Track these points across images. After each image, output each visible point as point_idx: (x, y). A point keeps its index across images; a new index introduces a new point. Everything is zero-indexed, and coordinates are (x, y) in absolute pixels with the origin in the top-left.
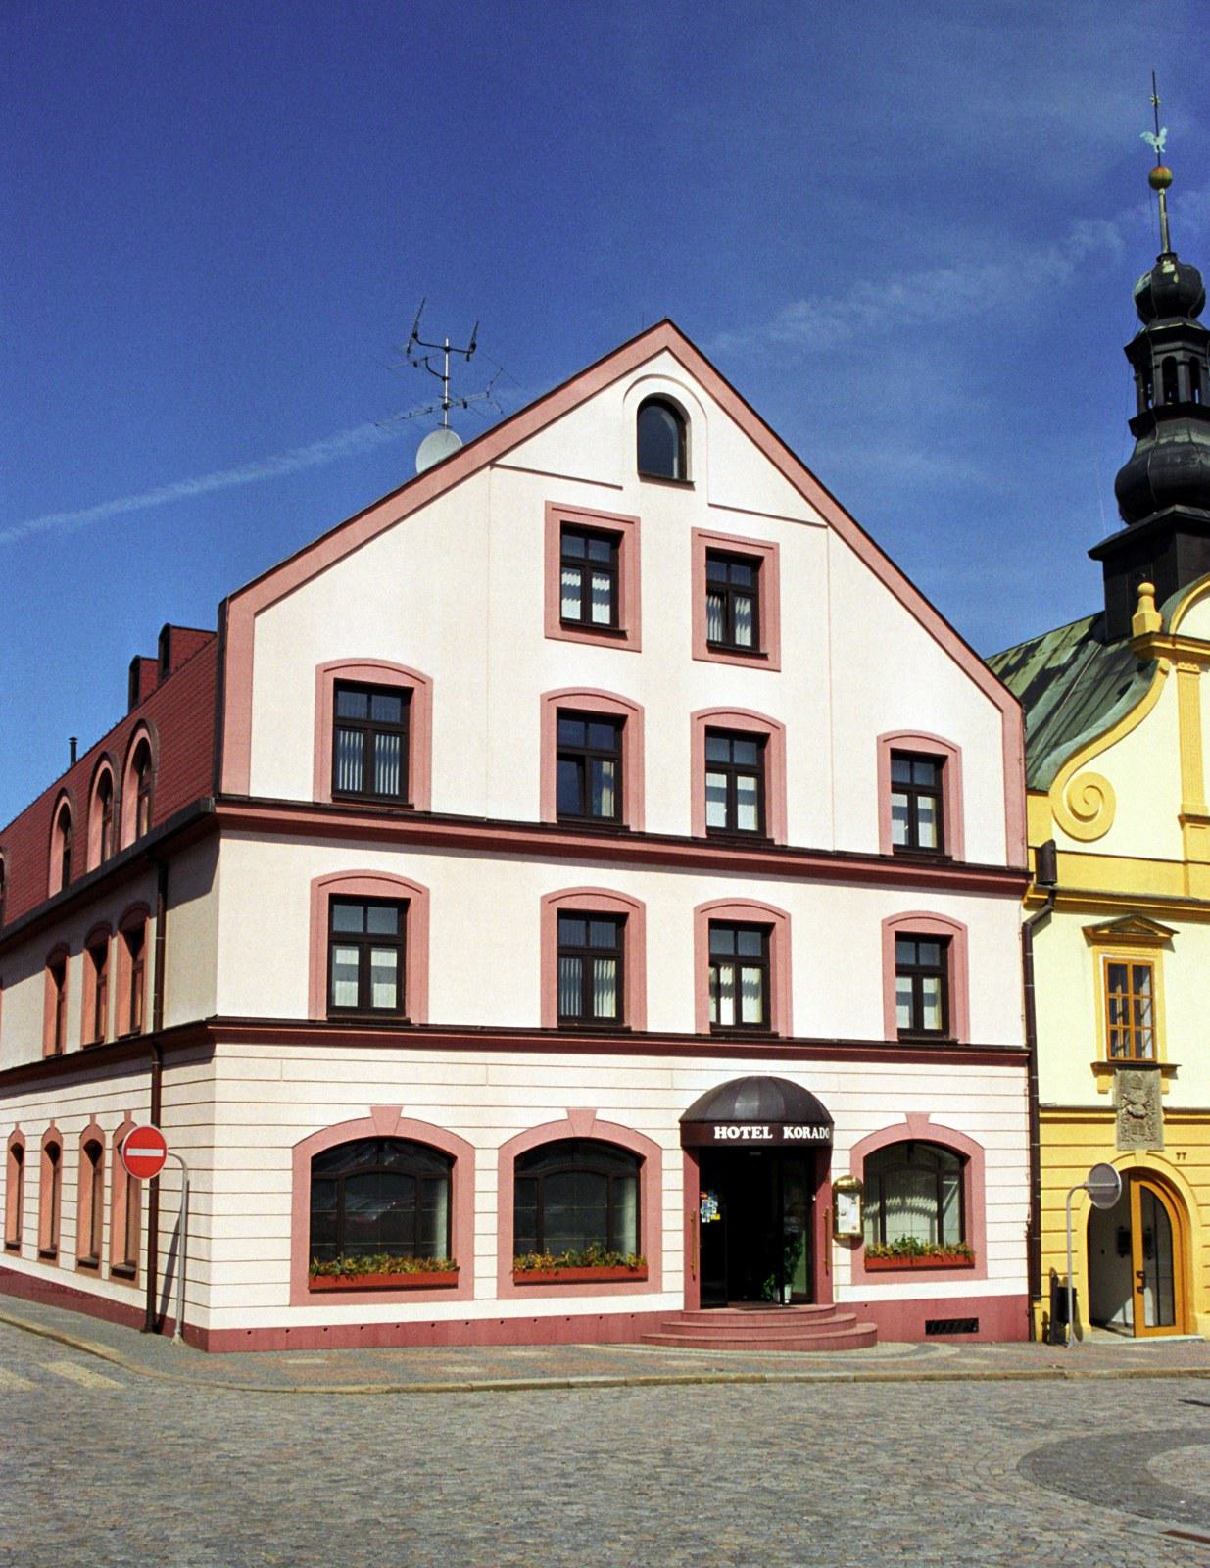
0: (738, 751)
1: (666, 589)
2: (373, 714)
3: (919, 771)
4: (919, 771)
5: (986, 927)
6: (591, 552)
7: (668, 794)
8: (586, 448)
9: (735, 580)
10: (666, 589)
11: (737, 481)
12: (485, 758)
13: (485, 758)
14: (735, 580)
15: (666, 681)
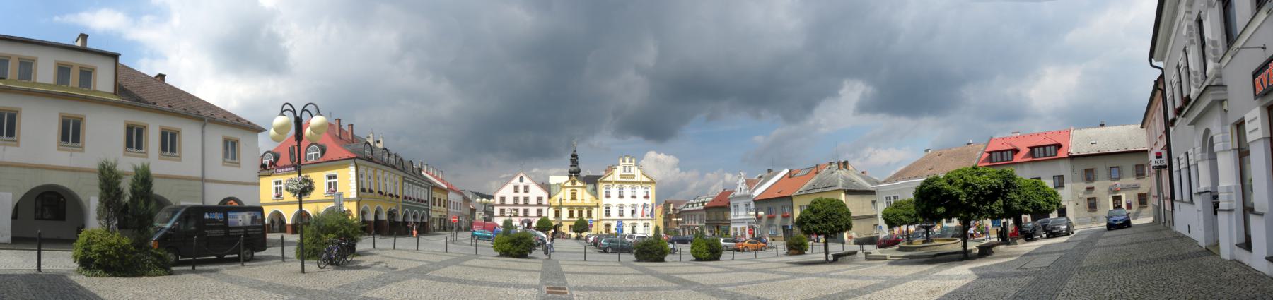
0: (526, 199)
1: (521, 189)
2: (503, 199)
3: (540, 199)
4: (540, 199)
5: (545, 210)
6: (516, 189)
7: (521, 201)
8: (516, 181)
9: (526, 188)
10: (521, 189)
11: (527, 181)
12: (509, 201)
13: (509, 201)
14: (526, 188)
15: (521, 195)
